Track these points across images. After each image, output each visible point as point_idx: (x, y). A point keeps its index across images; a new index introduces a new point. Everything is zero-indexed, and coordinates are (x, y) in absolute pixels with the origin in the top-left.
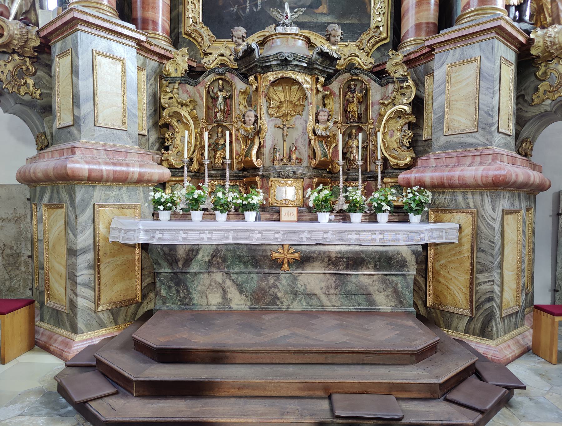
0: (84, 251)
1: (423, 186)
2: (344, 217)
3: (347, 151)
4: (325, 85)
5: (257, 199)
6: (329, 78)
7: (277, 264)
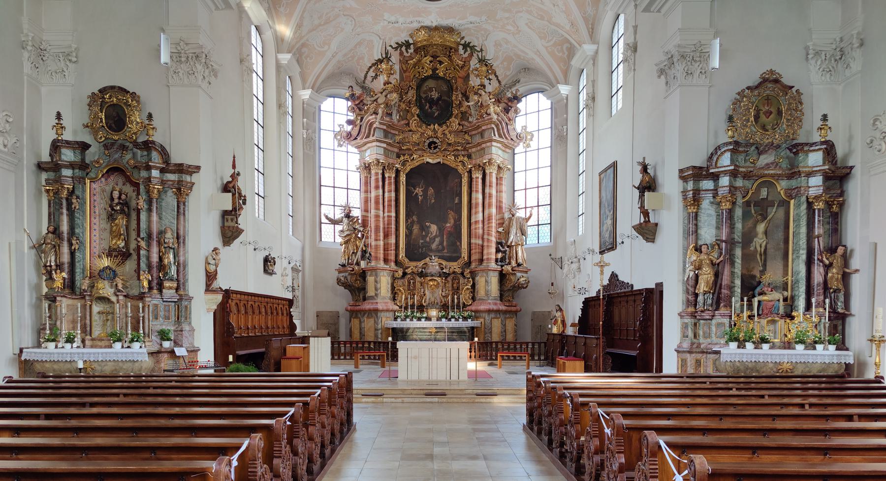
0: (380, 329)
1: (472, 311)
2: (450, 320)
3: (453, 301)
4: (445, 280)
5: (425, 315)
6: (446, 278)
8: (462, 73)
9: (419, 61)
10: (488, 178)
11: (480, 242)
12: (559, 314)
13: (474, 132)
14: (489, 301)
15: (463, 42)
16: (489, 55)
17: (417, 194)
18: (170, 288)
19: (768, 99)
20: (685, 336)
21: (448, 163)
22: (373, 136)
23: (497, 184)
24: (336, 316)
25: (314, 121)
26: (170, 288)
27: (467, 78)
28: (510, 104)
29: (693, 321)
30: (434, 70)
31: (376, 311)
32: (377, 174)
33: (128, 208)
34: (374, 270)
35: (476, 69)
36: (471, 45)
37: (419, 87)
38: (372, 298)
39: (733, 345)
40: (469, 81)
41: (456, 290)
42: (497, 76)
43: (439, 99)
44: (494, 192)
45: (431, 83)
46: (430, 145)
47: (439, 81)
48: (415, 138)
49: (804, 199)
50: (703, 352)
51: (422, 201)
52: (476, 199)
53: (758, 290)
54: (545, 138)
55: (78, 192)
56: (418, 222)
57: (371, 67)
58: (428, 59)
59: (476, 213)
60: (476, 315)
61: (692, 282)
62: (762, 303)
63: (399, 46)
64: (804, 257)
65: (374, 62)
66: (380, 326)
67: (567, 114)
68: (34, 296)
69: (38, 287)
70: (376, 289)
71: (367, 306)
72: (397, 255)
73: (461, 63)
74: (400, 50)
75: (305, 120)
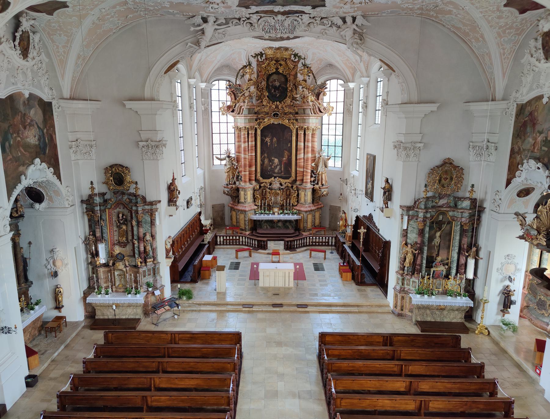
1: (297, 210)
3: (286, 202)
7: (275, 222)
8: (293, 73)
9: (269, 64)
10: (306, 136)
11: (302, 170)
12: (344, 215)
13: (299, 107)
14: (307, 206)
15: (294, 53)
16: (308, 62)
17: (267, 141)
18: (150, 262)
19: (446, 172)
20: (398, 283)
21: (285, 124)
22: (242, 114)
23: (312, 137)
24: (223, 206)
25: (208, 98)
26: (150, 262)
27: (295, 76)
28: (320, 90)
29: (402, 277)
30: (277, 69)
31: (245, 211)
32: (244, 134)
33: (127, 221)
34: (245, 189)
35: (301, 70)
36: (298, 55)
37: (268, 79)
38: (242, 203)
39: (418, 296)
40: (297, 77)
41: (288, 196)
42: (313, 74)
43: (279, 86)
44: (310, 145)
45: (275, 77)
46: (274, 115)
47: (280, 76)
48: (266, 109)
49: (459, 223)
50: (405, 293)
51: (270, 145)
52: (300, 146)
53: (434, 264)
54: (340, 108)
55: (103, 217)
56: (268, 157)
57: (240, 70)
58: (274, 62)
59: (300, 154)
60: (299, 213)
61: (403, 260)
62: (435, 272)
63: (257, 55)
64: (457, 251)
65: (242, 67)
66: (247, 219)
67: (353, 99)
68: (86, 264)
69: (87, 258)
70: (245, 199)
71: (240, 207)
72: (256, 176)
73: (293, 66)
74: (257, 58)
75: (203, 99)
